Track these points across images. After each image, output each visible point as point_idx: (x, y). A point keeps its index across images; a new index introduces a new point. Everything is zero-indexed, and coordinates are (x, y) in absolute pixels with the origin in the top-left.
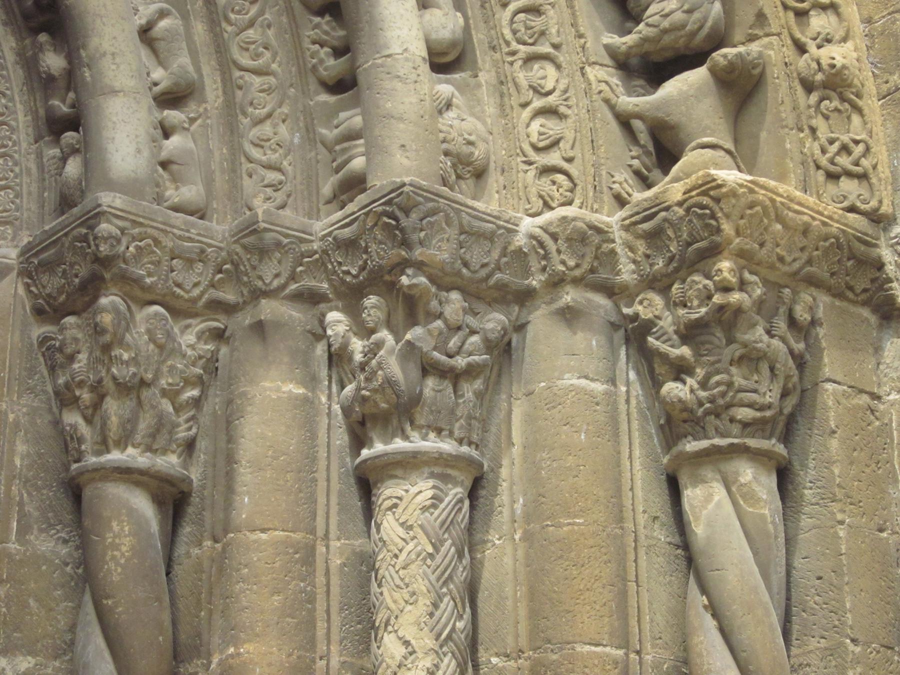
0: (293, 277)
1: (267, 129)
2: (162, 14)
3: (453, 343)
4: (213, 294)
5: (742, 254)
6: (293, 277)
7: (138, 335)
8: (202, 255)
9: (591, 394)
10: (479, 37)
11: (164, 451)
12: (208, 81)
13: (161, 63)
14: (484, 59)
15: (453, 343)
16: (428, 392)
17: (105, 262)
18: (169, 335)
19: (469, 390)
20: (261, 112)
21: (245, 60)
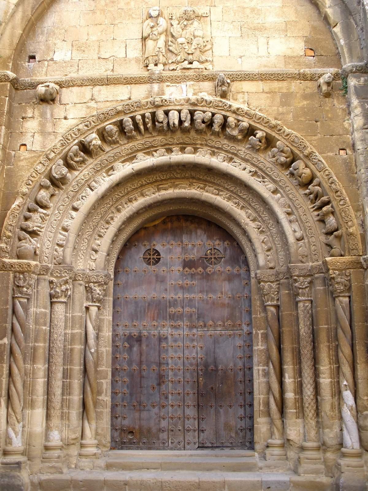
0: (284, 276)
1: (280, 253)
2: (265, 238)
3: (303, 284)
4: (276, 279)
5: (332, 269)
6: (284, 276)
7: (266, 287)
8: (273, 275)
9: (320, 289)
10: (304, 235)
11: (274, 302)
12: (273, 247)
13: (266, 245)
14: (305, 238)
15: (303, 284)
16: (300, 292)
17: (260, 279)
18: (271, 286)
19: (307, 290)
20: (279, 250)
21: (277, 243)
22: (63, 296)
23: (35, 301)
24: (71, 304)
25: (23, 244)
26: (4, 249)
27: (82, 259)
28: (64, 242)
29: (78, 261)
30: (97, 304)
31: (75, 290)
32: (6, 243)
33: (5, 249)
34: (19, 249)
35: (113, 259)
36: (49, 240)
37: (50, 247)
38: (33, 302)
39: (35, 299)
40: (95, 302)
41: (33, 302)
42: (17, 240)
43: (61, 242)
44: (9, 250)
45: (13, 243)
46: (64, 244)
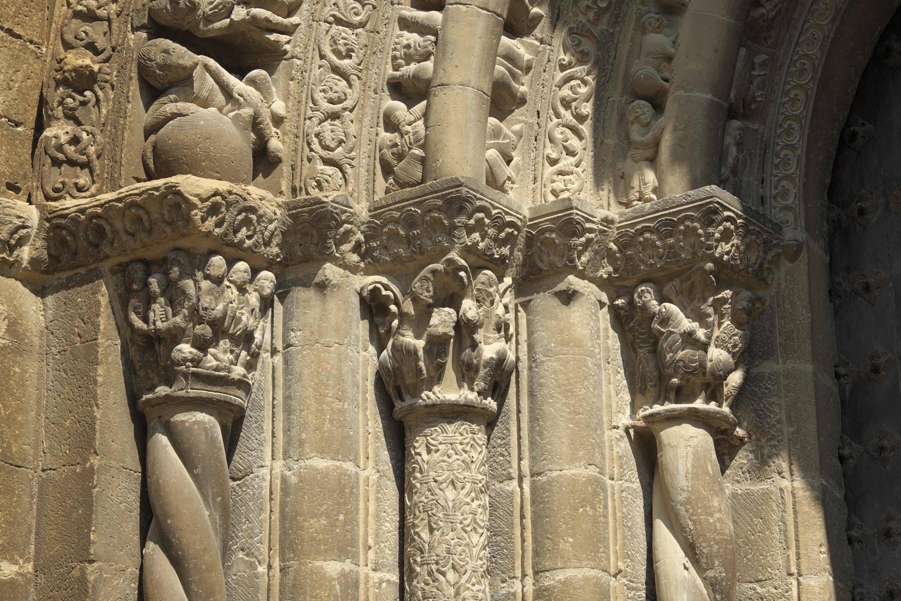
22: (450, 373)
23: (280, 417)
24: (525, 417)
25: (170, 108)
26: (60, 148)
27: (571, 153)
28: (429, 64)
29: (549, 170)
30: (699, 404)
31: (541, 334)
32: (71, 116)
33: (70, 149)
34: (152, 138)
35: (789, 132)
36: (336, 70)
37: (348, 103)
38: (267, 426)
39: (280, 409)
40: (680, 394)
41: (267, 426)
42: (134, 88)
43: (412, 68)
44: (92, 150)
45: (119, 112)
46: (430, 73)
